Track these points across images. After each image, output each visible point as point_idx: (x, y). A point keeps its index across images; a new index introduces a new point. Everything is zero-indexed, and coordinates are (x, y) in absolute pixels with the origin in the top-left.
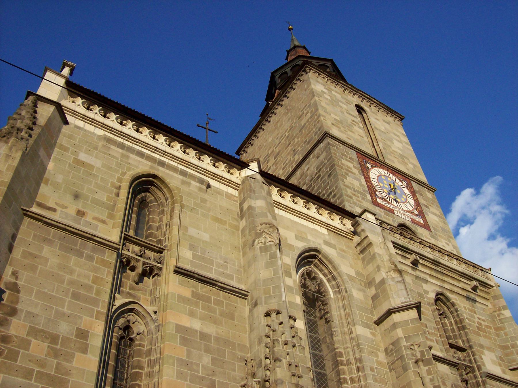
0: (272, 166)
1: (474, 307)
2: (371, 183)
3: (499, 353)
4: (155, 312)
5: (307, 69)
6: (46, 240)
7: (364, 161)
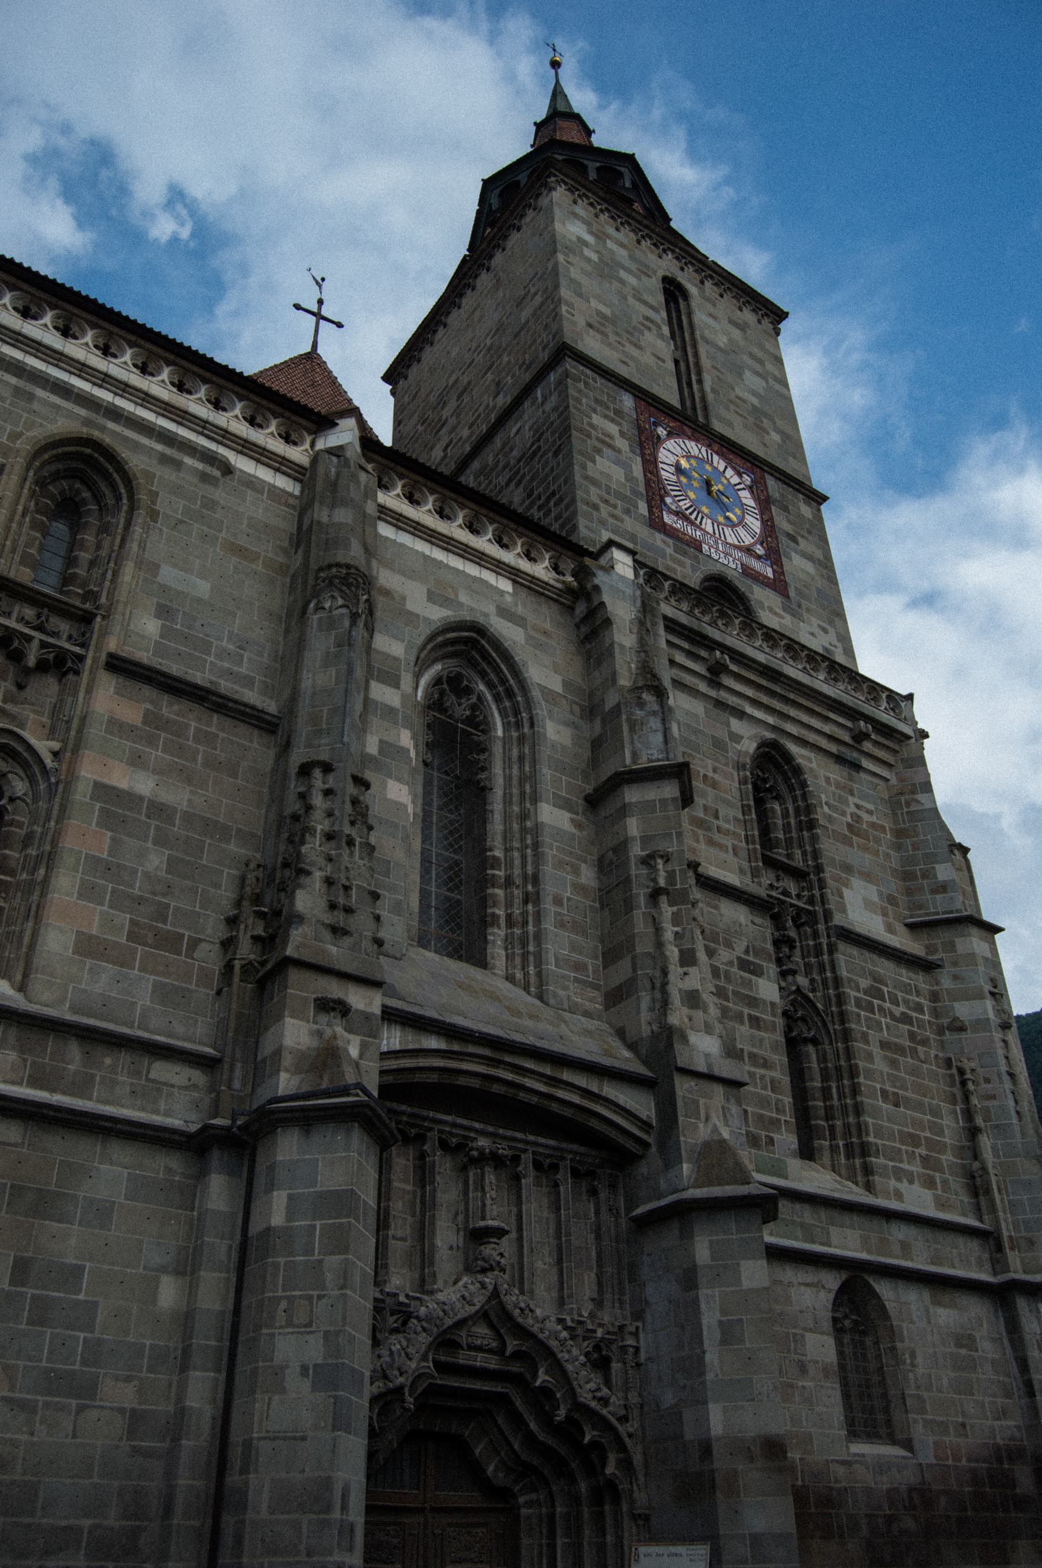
0: (452, 415)
1: (851, 780)
2: (658, 475)
3: (894, 886)
4: (56, 754)
5: (553, 179)
7: (652, 420)
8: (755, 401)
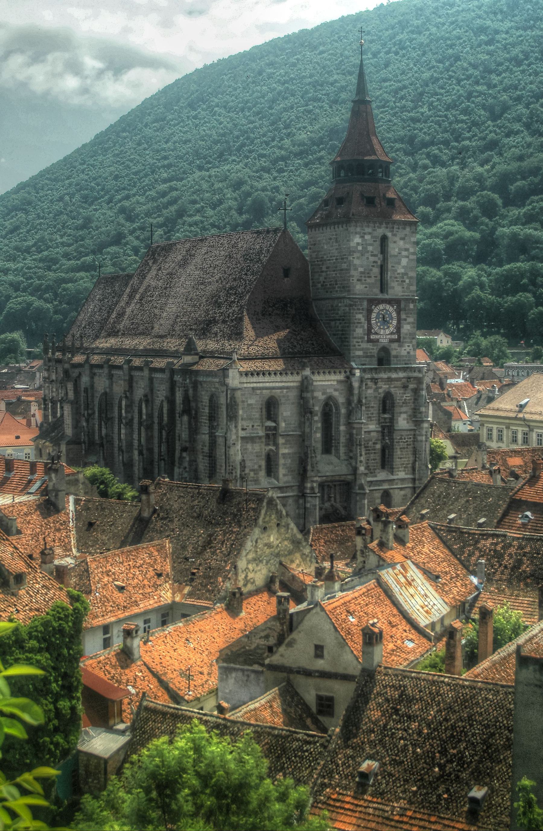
6: (247, 442)
8: (402, 271)
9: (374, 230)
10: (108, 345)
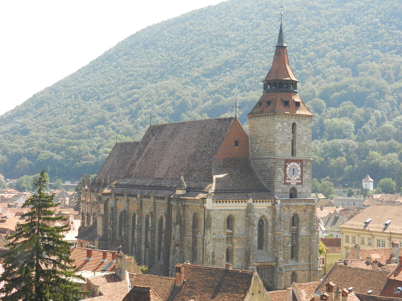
6: (216, 242)
9: (288, 120)
10: (126, 183)
